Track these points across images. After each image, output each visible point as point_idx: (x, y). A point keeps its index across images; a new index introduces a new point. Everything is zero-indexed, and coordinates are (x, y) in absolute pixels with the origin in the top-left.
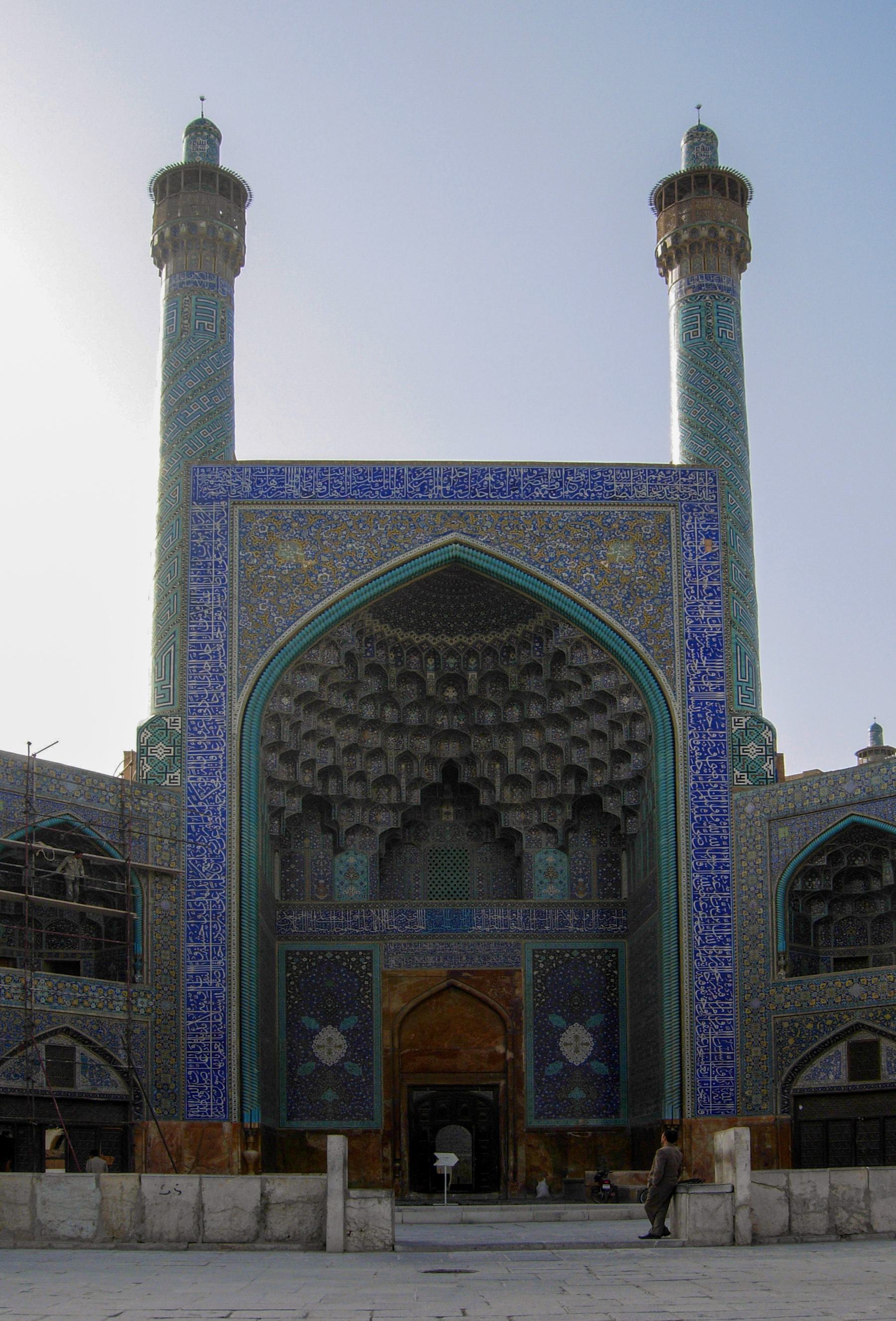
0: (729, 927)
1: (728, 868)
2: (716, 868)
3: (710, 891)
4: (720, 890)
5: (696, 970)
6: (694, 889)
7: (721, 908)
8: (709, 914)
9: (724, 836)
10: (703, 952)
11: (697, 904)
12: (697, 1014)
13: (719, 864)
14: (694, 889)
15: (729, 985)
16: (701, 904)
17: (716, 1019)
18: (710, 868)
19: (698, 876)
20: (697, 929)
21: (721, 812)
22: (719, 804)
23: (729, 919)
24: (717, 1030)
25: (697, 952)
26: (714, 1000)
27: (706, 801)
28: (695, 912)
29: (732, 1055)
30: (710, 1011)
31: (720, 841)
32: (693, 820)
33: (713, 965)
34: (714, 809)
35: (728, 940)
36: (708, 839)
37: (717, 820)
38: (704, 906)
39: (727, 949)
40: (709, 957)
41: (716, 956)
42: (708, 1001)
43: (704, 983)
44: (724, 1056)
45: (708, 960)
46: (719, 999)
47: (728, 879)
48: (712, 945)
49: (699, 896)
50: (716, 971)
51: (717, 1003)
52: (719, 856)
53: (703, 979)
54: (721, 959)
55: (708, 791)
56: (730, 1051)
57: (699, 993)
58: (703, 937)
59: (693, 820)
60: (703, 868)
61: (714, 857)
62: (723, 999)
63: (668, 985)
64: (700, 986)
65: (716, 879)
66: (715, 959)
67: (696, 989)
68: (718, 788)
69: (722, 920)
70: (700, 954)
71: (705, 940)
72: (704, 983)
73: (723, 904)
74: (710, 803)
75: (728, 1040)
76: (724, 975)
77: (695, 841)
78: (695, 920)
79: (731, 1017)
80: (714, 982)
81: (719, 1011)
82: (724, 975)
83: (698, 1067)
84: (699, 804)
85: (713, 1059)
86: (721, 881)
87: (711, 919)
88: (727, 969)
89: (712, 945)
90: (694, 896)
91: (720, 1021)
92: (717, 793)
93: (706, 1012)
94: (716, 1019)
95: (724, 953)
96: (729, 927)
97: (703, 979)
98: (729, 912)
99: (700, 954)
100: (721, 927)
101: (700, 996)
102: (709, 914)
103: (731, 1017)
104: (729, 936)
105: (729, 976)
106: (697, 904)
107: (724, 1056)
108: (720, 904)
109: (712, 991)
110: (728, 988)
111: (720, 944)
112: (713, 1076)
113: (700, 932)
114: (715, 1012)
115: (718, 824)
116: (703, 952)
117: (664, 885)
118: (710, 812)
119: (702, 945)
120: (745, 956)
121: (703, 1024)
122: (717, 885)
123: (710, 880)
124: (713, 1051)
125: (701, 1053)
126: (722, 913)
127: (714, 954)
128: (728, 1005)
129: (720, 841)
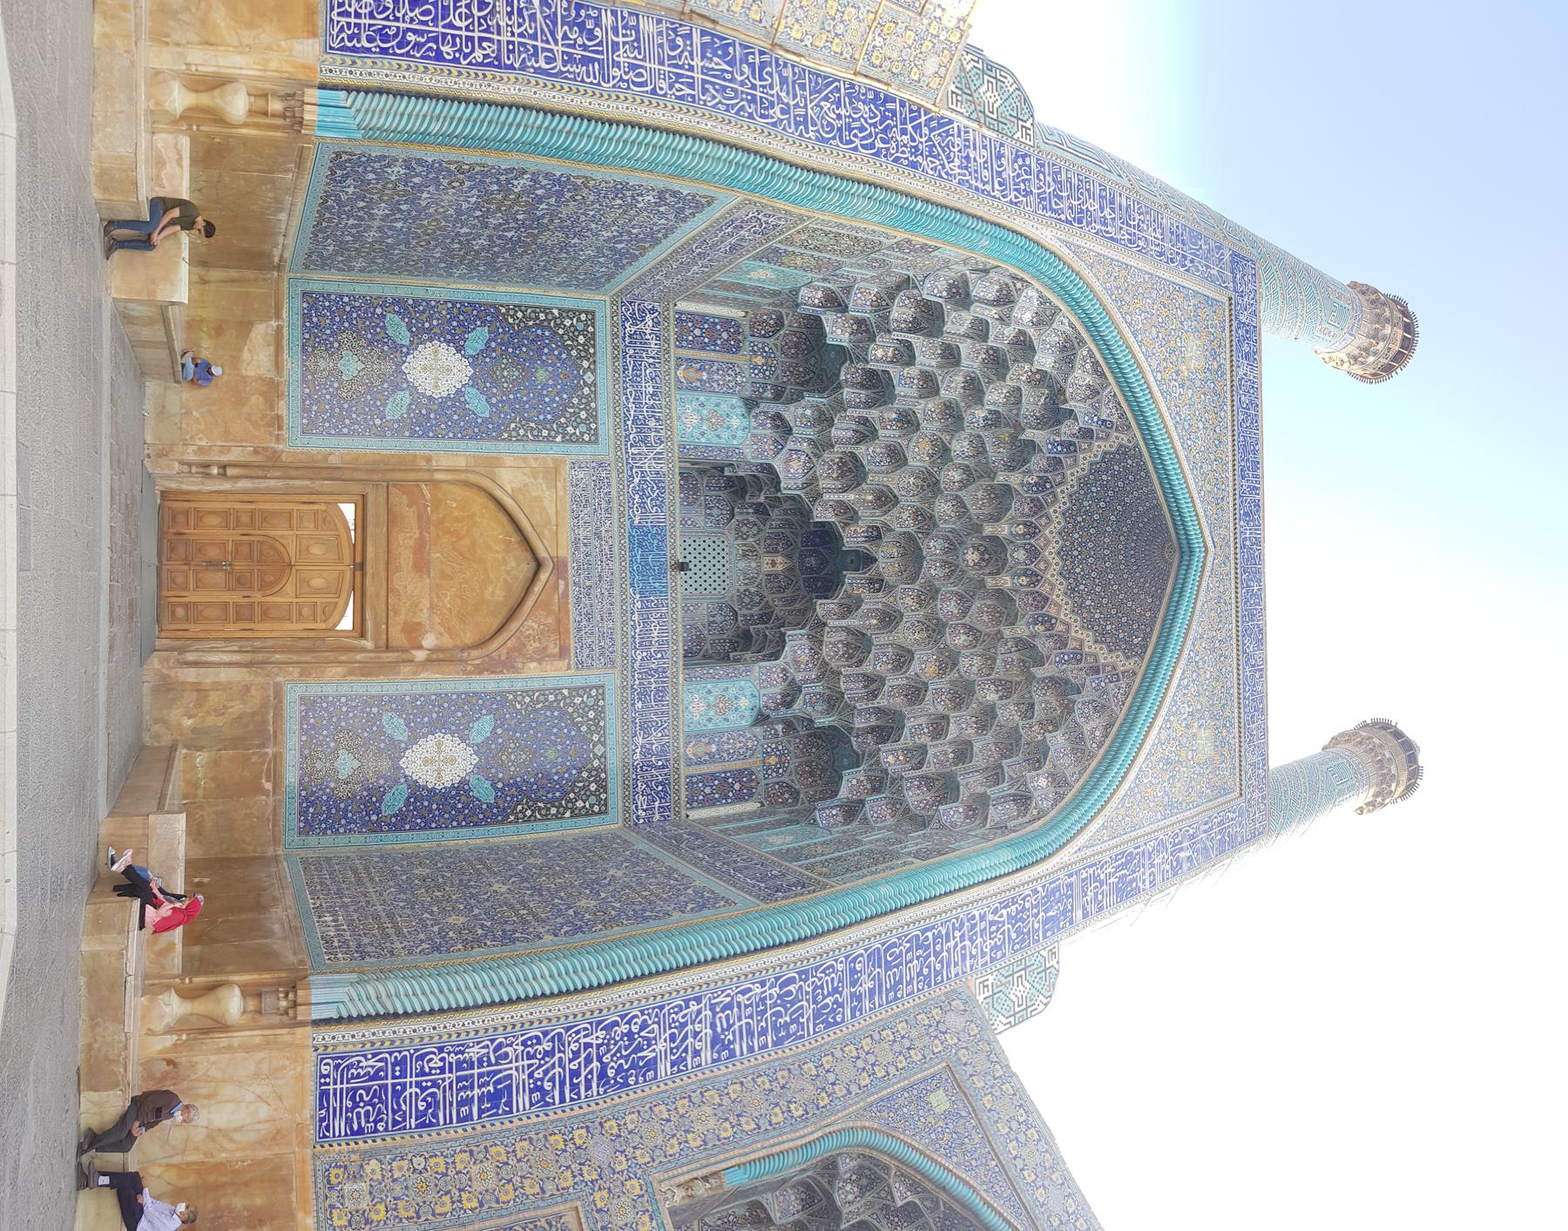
0: (751, 1049)
1: (853, 1016)
2: (853, 995)
3: (814, 998)
4: (817, 1015)
5: (661, 1008)
6: (817, 969)
7: (786, 1026)
8: (775, 1005)
9: (904, 990)
10: (699, 1012)
11: (791, 981)
12: (568, 1029)
14: (817, 969)
15: (631, 1080)
16: (791, 988)
17: (557, 1069)
18: (853, 984)
19: (840, 967)
20: (743, 993)
21: (937, 973)
23: (765, 1046)
24: (531, 1076)
25: (698, 1000)
26: (600, 1059)
27: (952, 943)
28: (777, 979)
29: (469, 1117)
30: (576, 1054)
31: (895, 988)
32: (924, 931)
33: (673, 1038)
34: (941, 962)
35: (725, 1053)
36: (896, 966)
37: (925, 971)
38: (789, 993)
39: (707, 1055)
40: (690, 1027)
41: (690, 1040)
42: (599, 1046)
43: (635, 1029)
44: (468, 1101)
45: (684, 1025)
46: (604, 1067)
47: (836, 1023)
48: (713, 1026)
49: (805, 981)
50: (661, 1046)
51: (595, 1064)
52: (872, 991)
53: (644, 1026)
54: (686, 1051)
55: (967, 943)
56: (481, 1111)
57: (616, 1024)
58: (729, 1006)
59: (924, 931)
60: (853, 971)
61: (870, 984)
62: (603, 1074)
63: (626, 959)
64: (628, 1023)
65: (836, 1002)
66: (685, 1038)
67: (622, 1017)
68: (972, 957)
69: (763, 1032)
70: (694, 1007)
71: (723, 1011)
72: (635, 1029)
73: (793, 1028)
74: (948, 951)
75: (509, 1104)
76: (652, 1064)
77: (894, 945)
78: (763, 984)
79: (562, 1100)
80: (639, 1049)
81: (575, 1074)
82: (652, 1064)
83: (441, 1050)
84: (947, 934)
85: (459, 1079)
86: (833, 1010)
87: (765, 1011)
88: (664, 1068)
89: (713, 1026)
90: (805, 972)
91: (552, 1080)
92: (964, 956)
93: (574, 1047)
94: (557, 1069)
95: (697, 1053)
96: (751, 1049)
99: (694, 1007)
100: (750, 1033)
101: (607, 1028)
102: (775, 1005)
103: (562, 1100)
104: (732, 1054)
105: (650, 1074)
106: (791, 981)
107: (468, 1101)
108: (792, 1022)
109: (619, 1050)
110: (626, 1078)
111: (715, 1040)
112: (418, 1084)
113: (740, 998)
115: (919, 974)
116: (699, 1012)
117: (821, 910)
118: (937, 954)
119: (712, 1009)
120: (696, 1097)
121: (547, 1046)
122: (827, 1006)
123: (835, 990)
124: (480, 1076)
125: (474, 1053)
126: (776, 1029)
127: (696, 1034)
128: (588, 1088)
129: (895, 988)
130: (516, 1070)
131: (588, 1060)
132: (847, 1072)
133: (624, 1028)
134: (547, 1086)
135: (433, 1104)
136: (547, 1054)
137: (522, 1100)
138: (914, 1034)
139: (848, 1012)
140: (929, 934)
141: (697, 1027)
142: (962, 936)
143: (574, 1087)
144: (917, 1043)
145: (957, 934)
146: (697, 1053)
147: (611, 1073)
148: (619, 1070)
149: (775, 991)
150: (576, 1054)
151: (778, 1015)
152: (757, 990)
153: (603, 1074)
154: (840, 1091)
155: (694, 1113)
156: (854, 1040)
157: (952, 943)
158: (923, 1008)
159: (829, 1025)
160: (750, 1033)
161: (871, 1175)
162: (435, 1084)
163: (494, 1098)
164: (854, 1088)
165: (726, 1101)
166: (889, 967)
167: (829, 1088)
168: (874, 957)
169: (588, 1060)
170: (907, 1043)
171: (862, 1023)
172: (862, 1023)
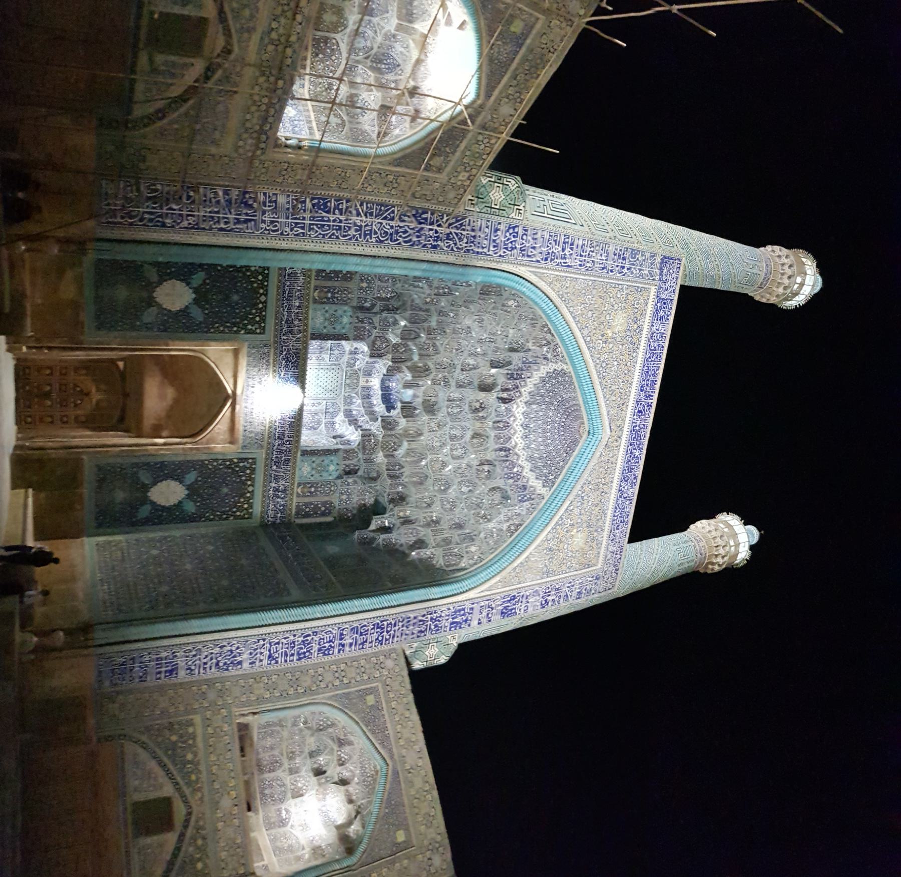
0: (286, 661)
1: (339, 652)
2: (340, 644)
4: (319, 650)
7: (304, 653)
9: (367, 645)
11: (309, 635)
13: (343, 646)
18: (341, 639)
21: (386, 640)
22: (394, 637)
25: (264, 640)
30: (206, 656)
31: (363, 644)
33: (251, 654)
35: (273, 662)
37: (380, 638)
39: (265, 662)
44: (160, 673)
46: (218, 662)
48: (270, 650)
50: (245, 656)
52: (351, 645)
58: (278, 643)
60: (342, 634)
61: (351, 641)
62: (217, 664)
69: (293, 655)
70: (261, 642)
73: (307, 654)
76: (240, 663)
78: (295, 636)
81: (205, 663)
88: (246, 665)
89: (270, 650)
95: (261, 661)
96: (286, 661)
97: (238, 648)
98: (300, 659)
99: (261, 642)
100: (286, 655)
101: (221, 647)
104: (277, 662)
106: (309, 635)
107: (160, 673)
111: (270, 656)
113: (284, 641)
114: (205, 661)
118: (388, 632)
119: (270, 643)
121: (194, 653)
123: (331, 641)
125: (164, 654)
126: (299, 654)
127: (261, 653)
129: (363, 644)
130: (181, 662)
131: (211, 659)
132: (329, 677)
133: (229, 648)
134: (193, 668)
135: (146, 673)
136: (195, 656)
137: (182, 673)
138: (367, 666)
139: (336, 650)
140: (385, 623)
141: (262, 650)
142: (403, 626)
143: (205, 668)
144: (367, 671)
145: (401, 624)
146: (261, 661)
147: (221, 664)
148: (225, 664)
149: (301, 639)
150: (206, 656)
151: (301, 648)
152: (292, 638)
153: (217, 664)
154: (323, 685)
155: (256, 685)
156: (336, 663)
157: (397, 628)
158: (376, 655)
159: (325, 654)
160: (286, 655)
162: (146, 666)
163: (171, 672)
164: (330, 685)
165: (270, 682)
166: (361, 634)
167: (318, 683)
168: (354, 630)
169: (211, 659)
170: (363, 670)
171: (342, 656)
172: (342, 656)
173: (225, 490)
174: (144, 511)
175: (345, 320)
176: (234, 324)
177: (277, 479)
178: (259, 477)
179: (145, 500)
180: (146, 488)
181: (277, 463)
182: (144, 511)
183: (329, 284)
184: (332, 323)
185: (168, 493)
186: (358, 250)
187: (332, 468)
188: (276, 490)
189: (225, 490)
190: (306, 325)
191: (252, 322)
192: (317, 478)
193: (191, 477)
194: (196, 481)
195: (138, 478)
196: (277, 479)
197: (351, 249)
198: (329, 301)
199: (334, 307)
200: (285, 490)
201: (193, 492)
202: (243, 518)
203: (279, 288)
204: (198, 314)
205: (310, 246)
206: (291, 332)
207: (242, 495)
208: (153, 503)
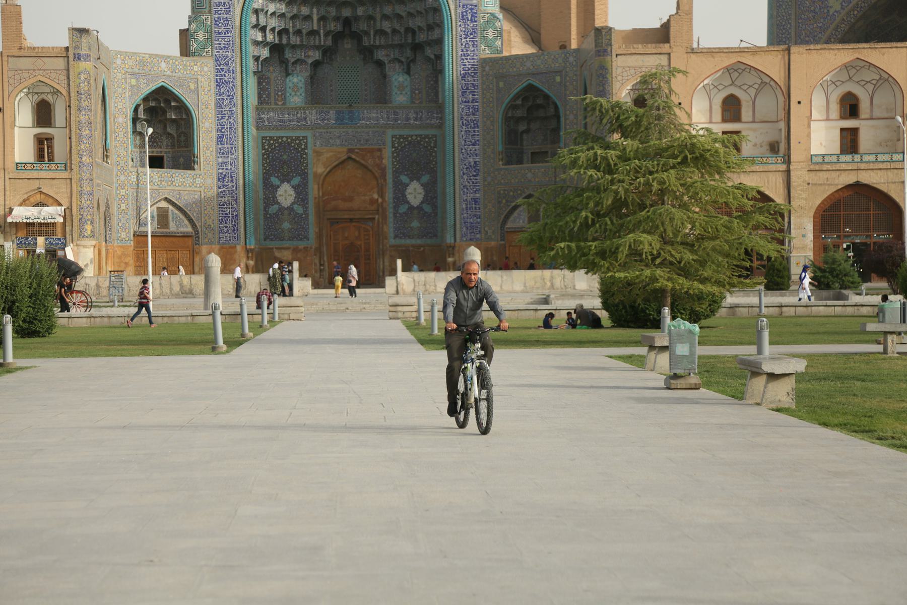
4: (474, 114)
39: (477, 147)
62: (474, 176)
63: (449, 169)
76: (475, 162)
88: (477, 159)
111: (473, 145)
130: (470, 197)
137: (478, 195)
153: (474, 176)
161: (512, 107)
173: (415, 155)
174: (427, 208)
175: (295, 80)
176: (302, 157)
177: (408, 119)
178: (405, 132)
179: (419, 208)
180: (411, 208)
181: (396, 120)
182: (427, 208)
183: (272, 94)
184: (298, 90)
185: (415, 193)
186: (240, 116)
187: (401, 79)
188: (416, 119)
189: (415, 155)
190: (300, 108)
191: (300, 144)
192: (408, 90)
193: (404, 179)
194: (407, 175)
195: (405, 213)
196: (408, 119)
197: (240, 121)
198: (284, 94)
199: (288, 89)
200: (416, 113)
201: (415, 177)
202: (436, 141)
203: (277, 129)
204: (296, 180)
205: (240, 143)
206: (305, 119)
207: (419, 142)
208: (422, 203)
